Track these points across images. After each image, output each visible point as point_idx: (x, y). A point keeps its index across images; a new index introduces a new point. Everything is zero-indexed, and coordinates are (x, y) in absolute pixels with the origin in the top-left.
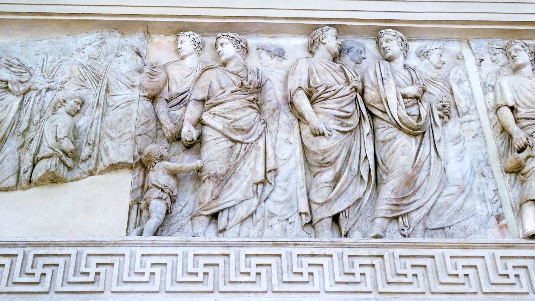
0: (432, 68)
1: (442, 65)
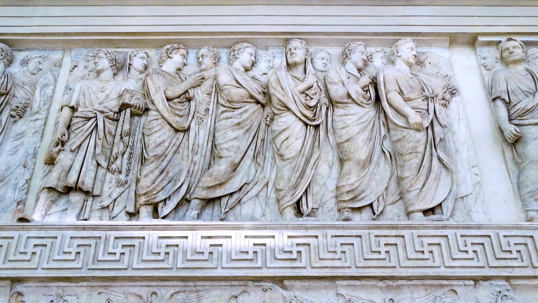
0: (28, 74)
1: (38, 71)
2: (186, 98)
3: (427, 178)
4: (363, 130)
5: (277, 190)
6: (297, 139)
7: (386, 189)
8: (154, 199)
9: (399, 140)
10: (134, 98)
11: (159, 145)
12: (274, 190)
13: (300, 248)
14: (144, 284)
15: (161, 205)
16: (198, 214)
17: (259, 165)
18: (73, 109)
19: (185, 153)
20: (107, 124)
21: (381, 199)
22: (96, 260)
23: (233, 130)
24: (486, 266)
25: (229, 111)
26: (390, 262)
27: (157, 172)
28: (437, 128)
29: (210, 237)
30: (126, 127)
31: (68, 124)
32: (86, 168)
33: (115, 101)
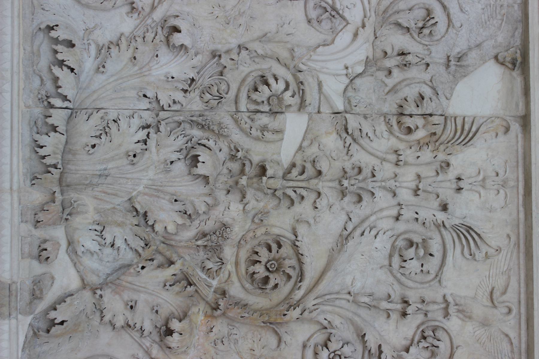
14: (523, 296)
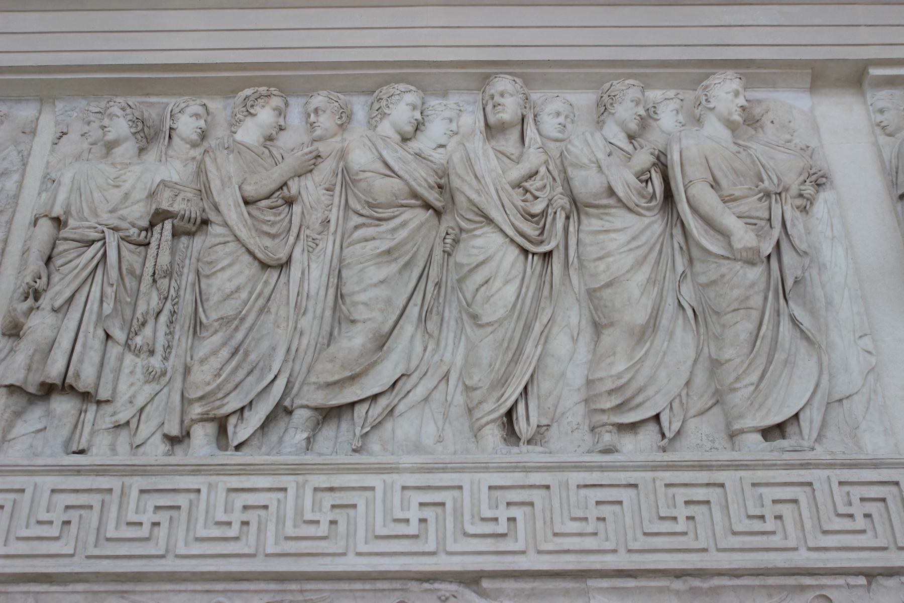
2: (283, 198)
3: (769, 362)
4: (639, 263)
5: (468, 389)
6: (506, 282)
7: (687, 384)
8: (219, 407)
9: (713, 283)
10: (179, 198)
11: (229, 297)
12: (460, 387)
13: (515, 512)
14: (198, 587)
15: (232, 420)
16: (308, 439)
17: (431, 336)
18: (59, 222)
19: (283, 312)
20: (125, 253)
21: (676, 405)
22: (101, 537)
23: (376, 264)
24: (892, 546)
25: (370, 225)
26: (697, 538)
27: (225, 353)
28: (788, 257)
29: (331, 489)
30: (164, 259)
31: (48, 253)
32: (84, 345)
33: (142, 204)
